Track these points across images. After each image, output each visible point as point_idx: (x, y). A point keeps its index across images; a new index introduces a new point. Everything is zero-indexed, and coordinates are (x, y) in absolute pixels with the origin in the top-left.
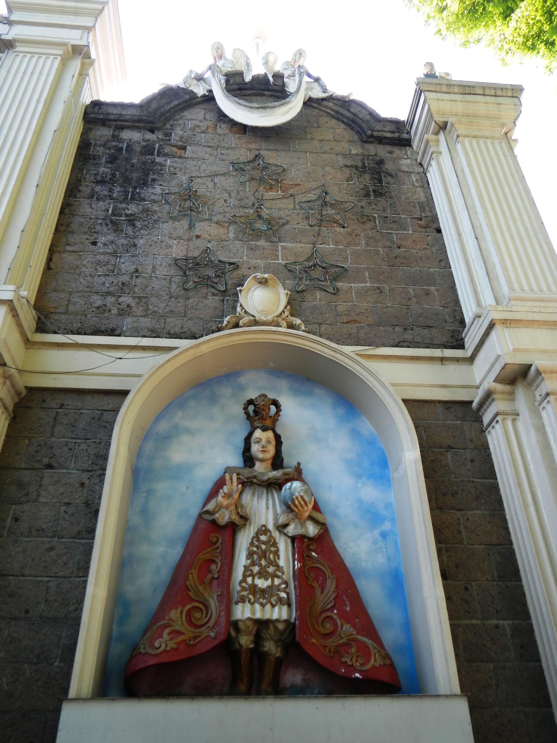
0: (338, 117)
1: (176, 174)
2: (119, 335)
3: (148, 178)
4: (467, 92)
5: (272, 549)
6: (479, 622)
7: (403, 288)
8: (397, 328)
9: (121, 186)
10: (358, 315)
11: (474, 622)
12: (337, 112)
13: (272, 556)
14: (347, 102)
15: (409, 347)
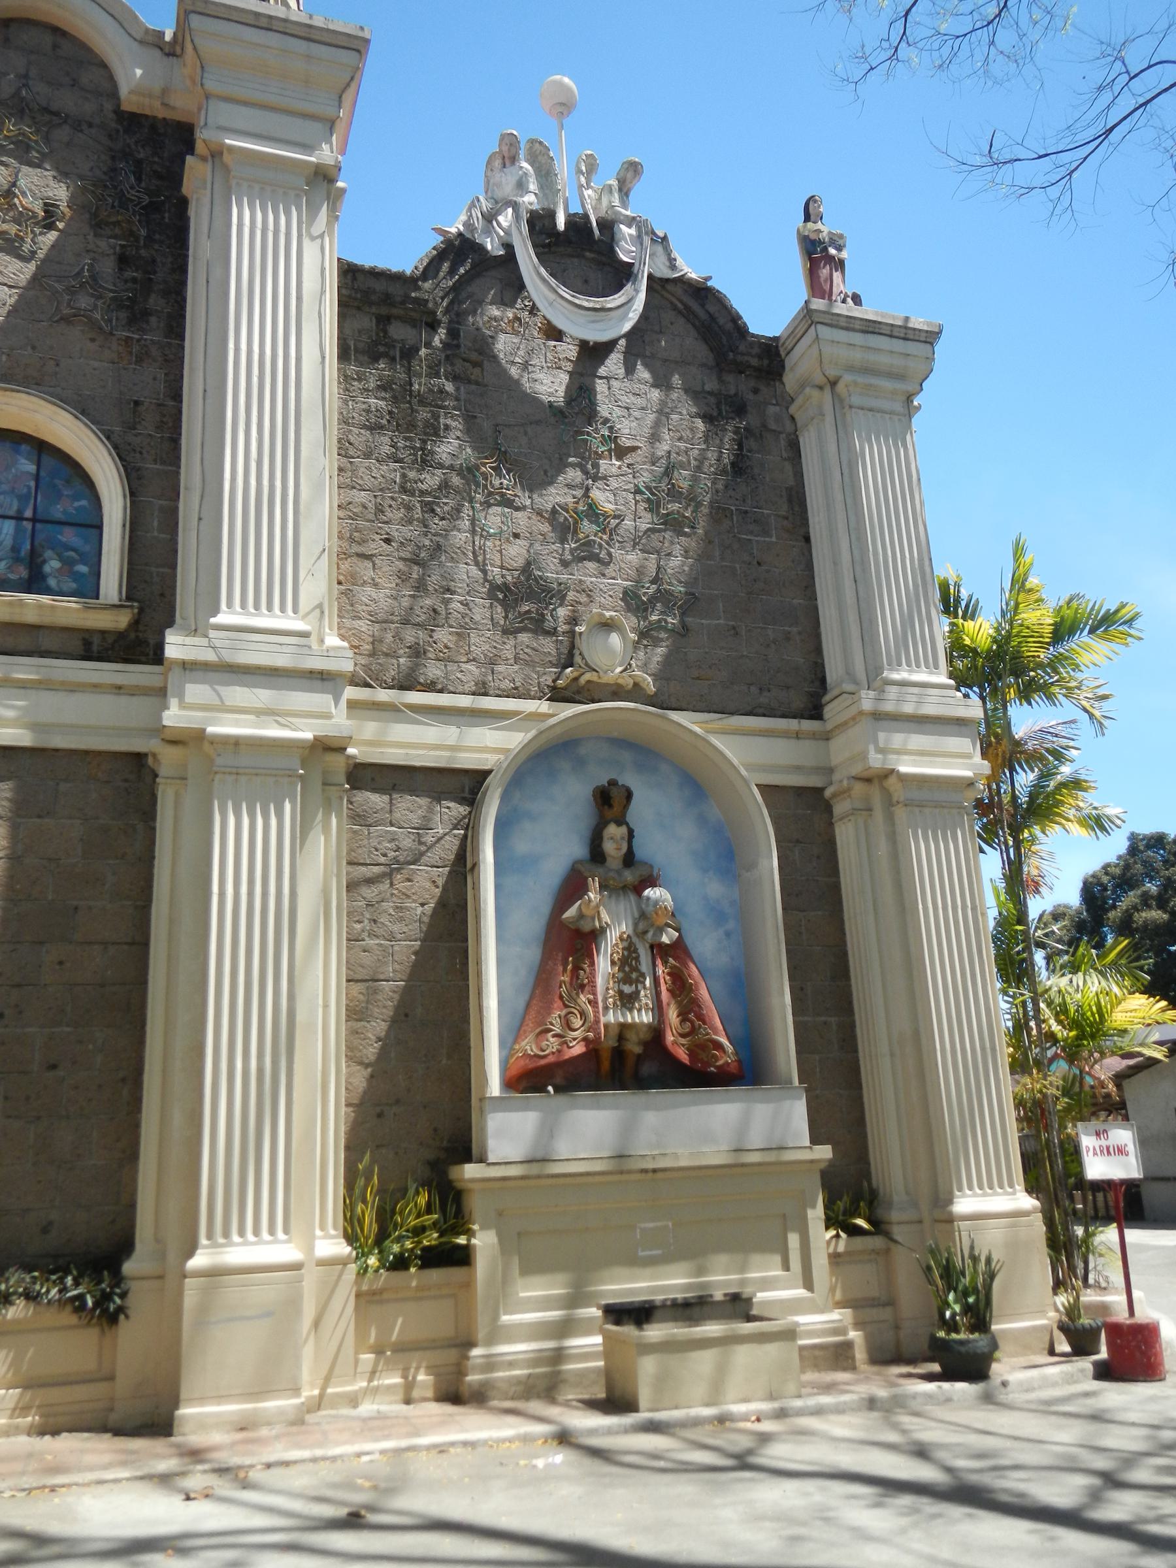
0: (687, 314)
1: (475, 417)
2: (441, 691)
3: (439, 423)
4: (870, 329)
5: (634, 955)
6: (809, 1019)
7: (762, 628)
8: (753, 688)
9: (406, 439)
10: (710, 667)
11: (806, 1018)
12: (686, 307)
13: (634, 963)
14: (703, 289)
15: (764, 715)
